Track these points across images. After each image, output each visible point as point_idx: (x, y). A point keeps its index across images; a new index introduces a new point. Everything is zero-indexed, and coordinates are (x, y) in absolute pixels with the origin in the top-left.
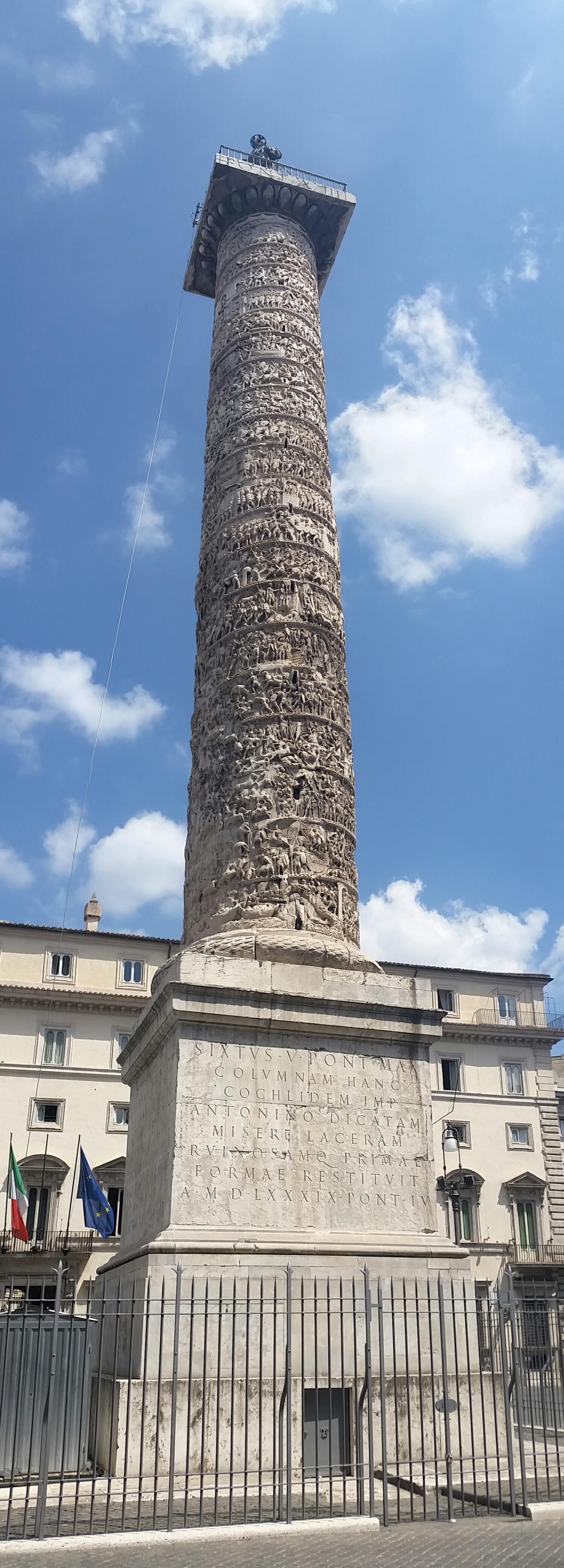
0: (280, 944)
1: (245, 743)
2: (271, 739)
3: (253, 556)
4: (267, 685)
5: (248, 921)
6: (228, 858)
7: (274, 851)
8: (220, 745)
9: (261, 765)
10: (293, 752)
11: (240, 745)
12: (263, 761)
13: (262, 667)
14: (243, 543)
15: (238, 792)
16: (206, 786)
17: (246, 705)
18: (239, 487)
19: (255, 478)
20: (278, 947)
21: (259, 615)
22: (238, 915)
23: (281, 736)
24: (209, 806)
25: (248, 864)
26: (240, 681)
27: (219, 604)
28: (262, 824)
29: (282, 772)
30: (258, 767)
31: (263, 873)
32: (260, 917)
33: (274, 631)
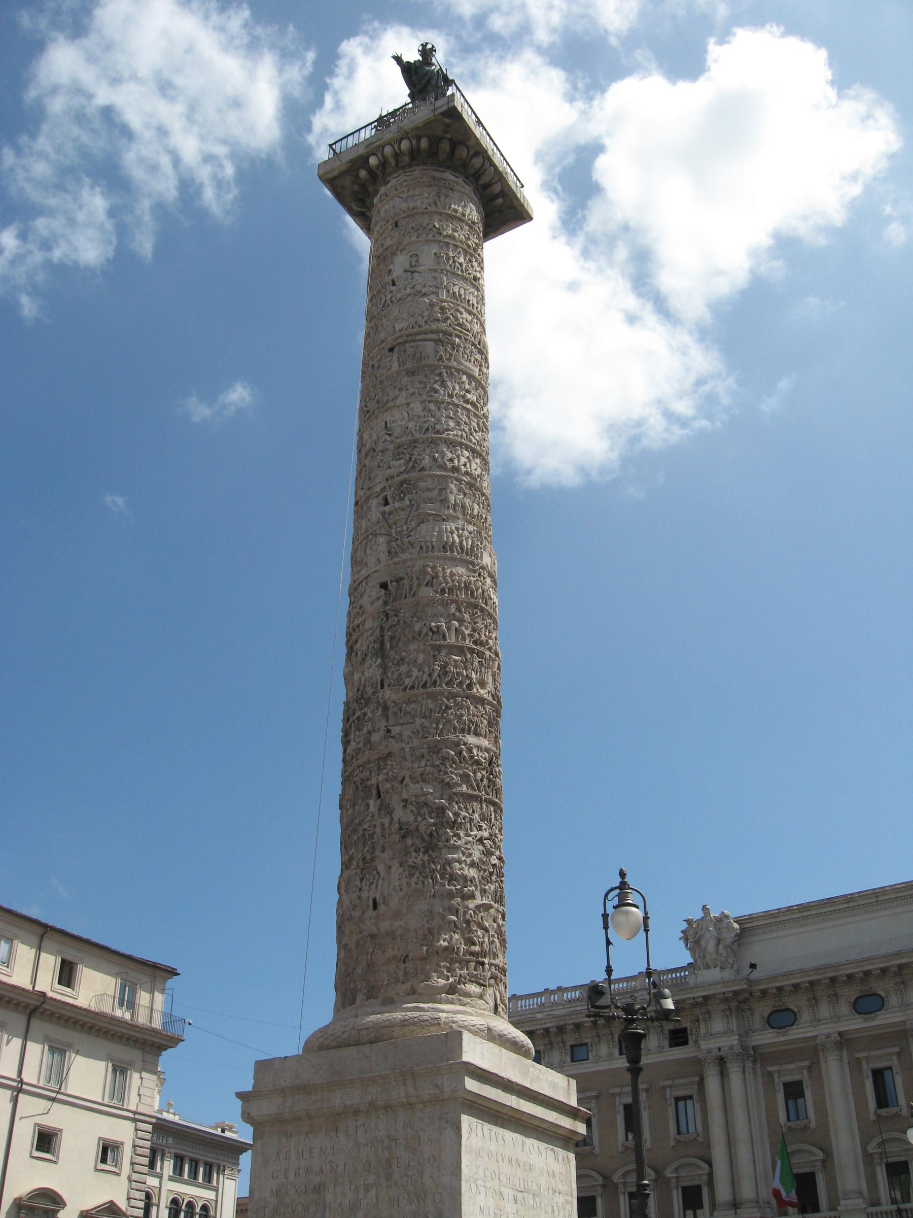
0: (505, 1032)
1: (456, 814)
2: (476, 818)
3: (460, 612)
4: (473, 760)
5: (462, 998)
6: (440, 930)
7: (479, 933)
8: (426, 804)
9: (470, 842)
10: (491, 837)
11: (451, 814)
12: (470, 839)
13: (471, 739)
14: (451, 590)
15: (449, 863)
16: (409, 842)
17: (456, 774)
18: (444, 520)
19: (458, 518)
20: (505, 1035)
21: (467, 682)
22: (452, 990)
23: (483, 818)
24: (413, 867)
25: (460, 940)
26: (449, 746)
27: (422, 647)
28: (472, 904)
29: (484, 854)
30: (466, 843)
31: (472, 954)
32: (472, 997)
33: (477, 703)
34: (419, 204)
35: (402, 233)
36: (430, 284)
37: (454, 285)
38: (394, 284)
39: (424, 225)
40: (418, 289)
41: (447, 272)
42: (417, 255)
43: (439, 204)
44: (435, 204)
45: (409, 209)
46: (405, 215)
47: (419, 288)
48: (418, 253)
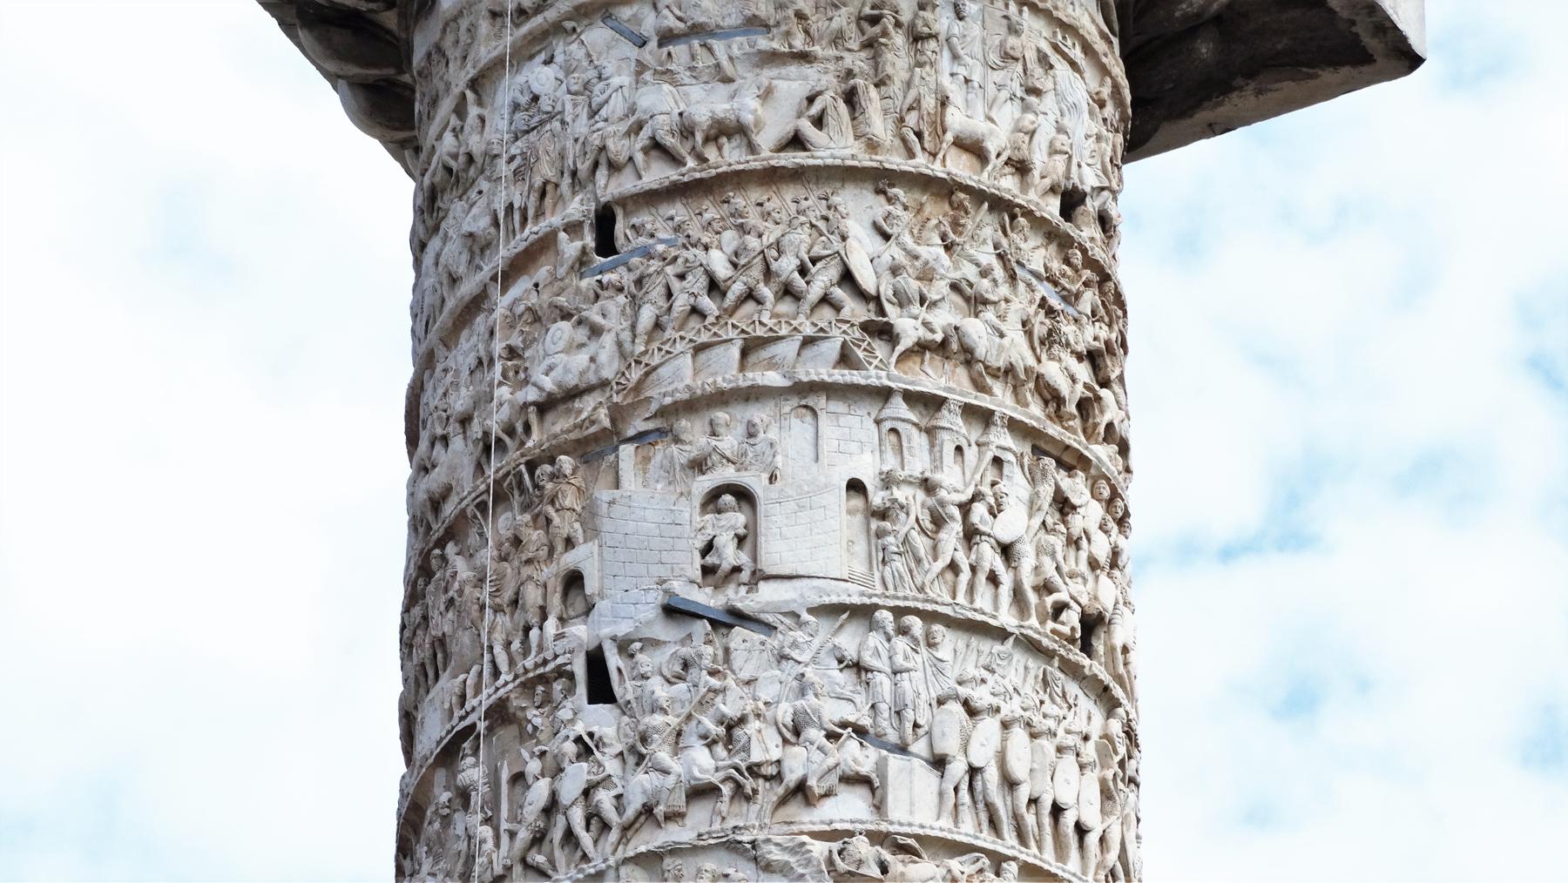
34: (748, 106)
35: (647, 316)
36: (834, 712)
37: (972, 712)
38: (601, 690)
39: (787, 266)
40: (756, 756)
41: (929, 617)
42: (744, 496)
43: (872, 100)
44: (851, 97)
45: (686, 131)
46: (657, 174)
47: (764, 745)
48: (754, 481)
